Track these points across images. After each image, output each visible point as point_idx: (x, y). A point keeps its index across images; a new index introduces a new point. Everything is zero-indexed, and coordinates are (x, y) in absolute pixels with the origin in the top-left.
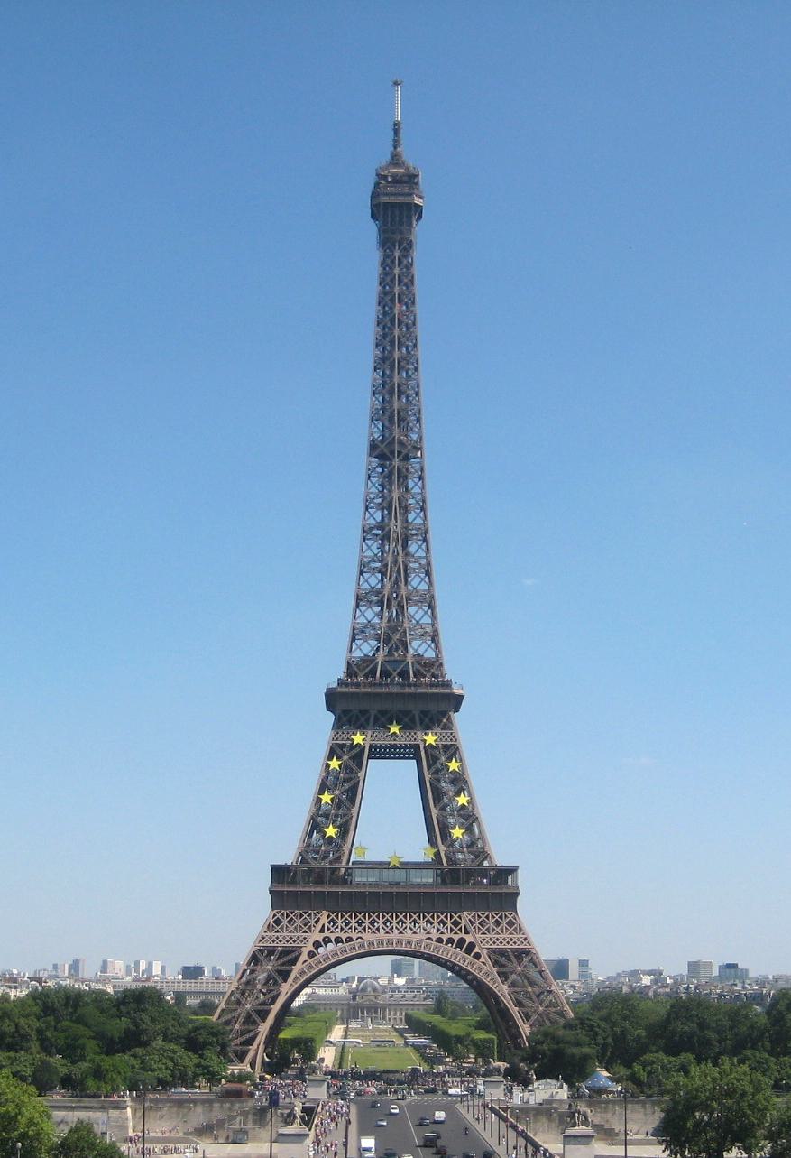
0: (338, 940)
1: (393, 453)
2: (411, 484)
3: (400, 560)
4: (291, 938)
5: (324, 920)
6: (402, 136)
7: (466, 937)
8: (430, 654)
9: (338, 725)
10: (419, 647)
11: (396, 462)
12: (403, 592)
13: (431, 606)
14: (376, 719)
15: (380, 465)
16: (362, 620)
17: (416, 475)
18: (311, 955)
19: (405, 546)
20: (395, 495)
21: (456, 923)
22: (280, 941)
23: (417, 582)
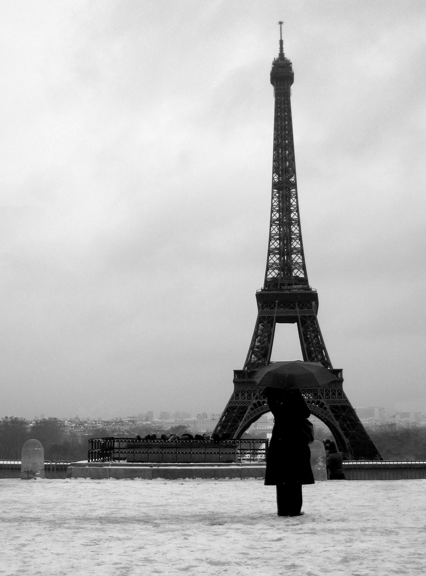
1: (283, 187)
2: (291, 201)
3: (287, 235)
4: (243, 402)
5: (258, 394)
6: (284, 46)
7: (320, 400)
8: (302, 276)
10: (298, 273)
11: (284, 191)
12: (289, 248)
13: (302, 254)
15: (278, 193)
16: (271, 261)
18: (252, 409)
19: (290, 229)
20: (285, 205)
21: (316, 394)
22: (239, 403)
23: (295, 244)
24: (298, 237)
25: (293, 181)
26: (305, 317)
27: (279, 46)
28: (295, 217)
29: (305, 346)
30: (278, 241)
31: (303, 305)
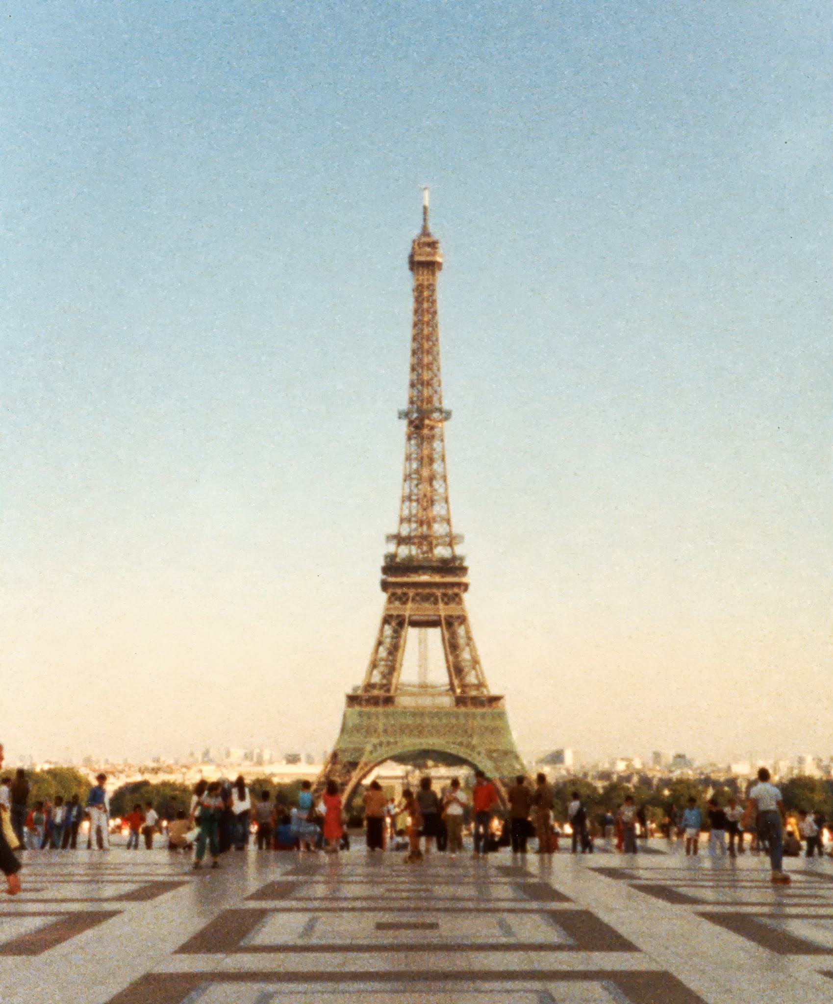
0: (388, 743)
3: (429, 494)
9: (390, 601)
14: (413, 600)
18: (371, 752)
19: (431, 485)
23: (438, 509)
26: (451, 617)
27: (421, 217)
29: (451, 658)
31: (449, 599)
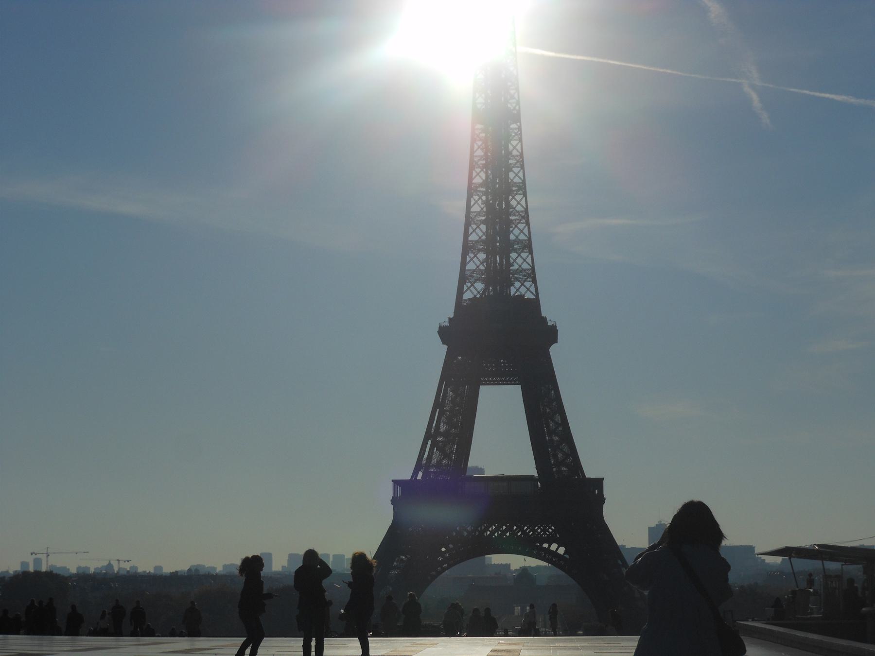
2: (511, 147)
8: (529, 295)
16: (470, 266)
17: (516, 137)
24: (523, 217)
25: (515, 109)
28: (517, 180)
30: (483, 227)
